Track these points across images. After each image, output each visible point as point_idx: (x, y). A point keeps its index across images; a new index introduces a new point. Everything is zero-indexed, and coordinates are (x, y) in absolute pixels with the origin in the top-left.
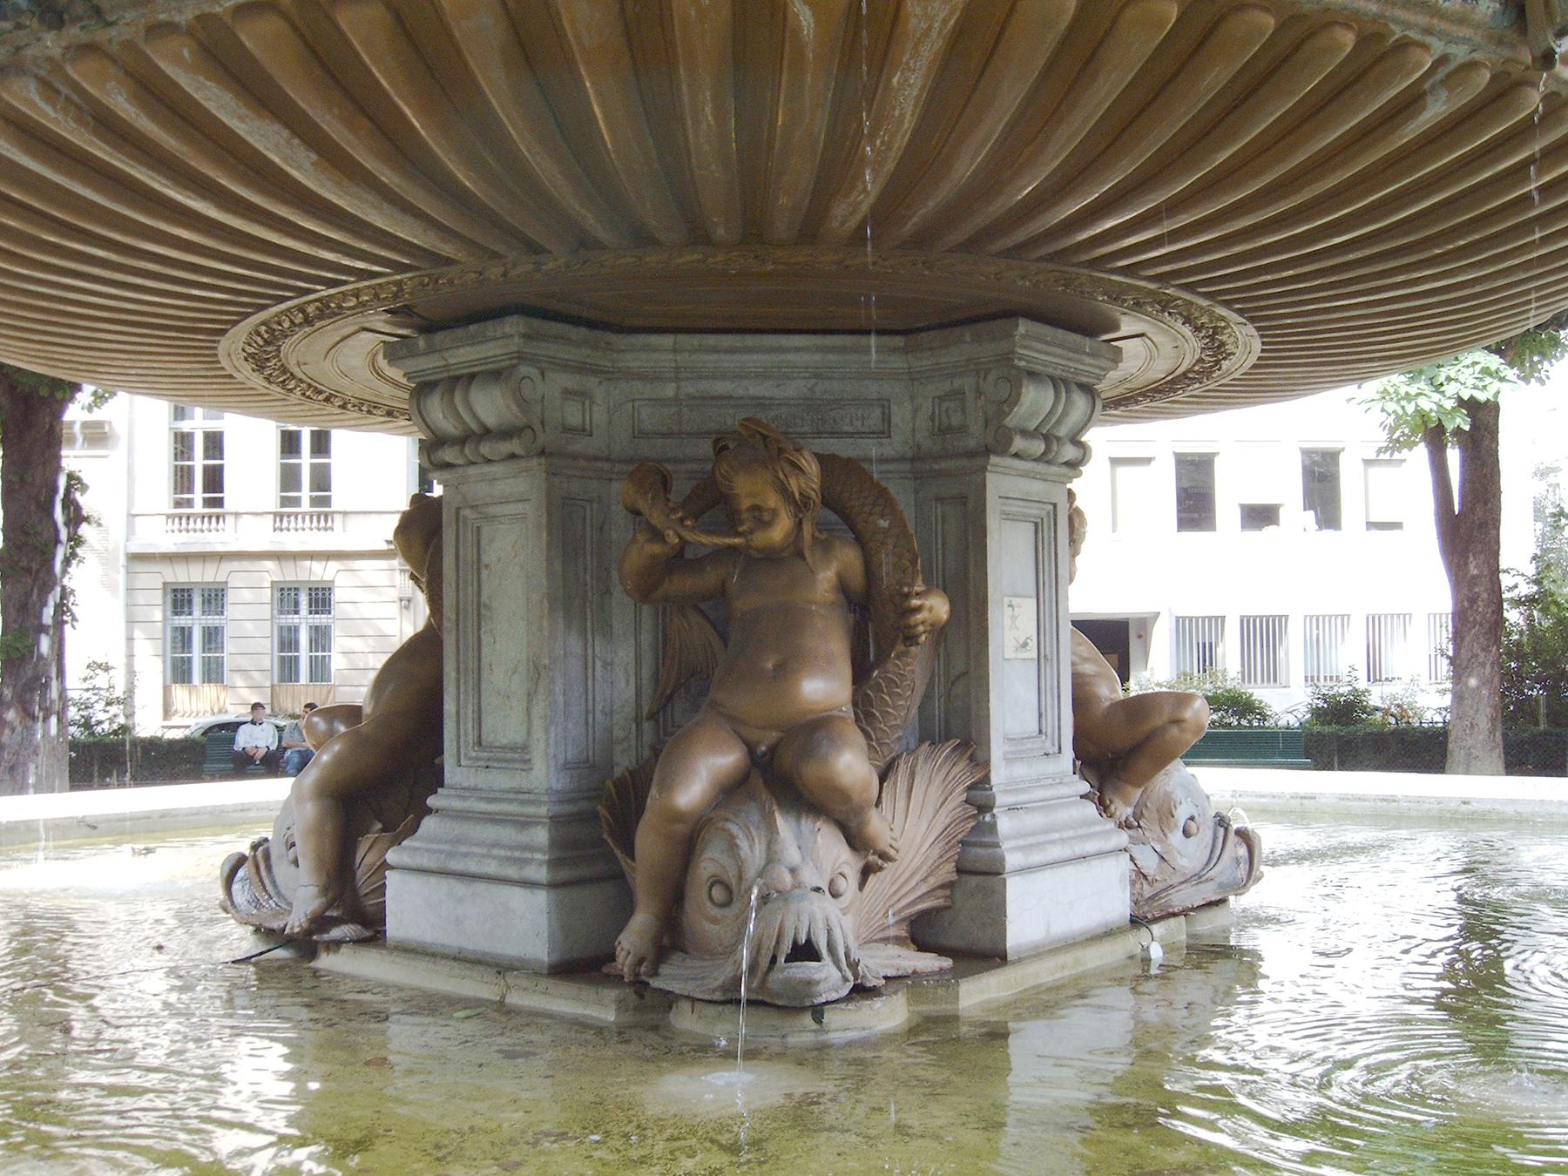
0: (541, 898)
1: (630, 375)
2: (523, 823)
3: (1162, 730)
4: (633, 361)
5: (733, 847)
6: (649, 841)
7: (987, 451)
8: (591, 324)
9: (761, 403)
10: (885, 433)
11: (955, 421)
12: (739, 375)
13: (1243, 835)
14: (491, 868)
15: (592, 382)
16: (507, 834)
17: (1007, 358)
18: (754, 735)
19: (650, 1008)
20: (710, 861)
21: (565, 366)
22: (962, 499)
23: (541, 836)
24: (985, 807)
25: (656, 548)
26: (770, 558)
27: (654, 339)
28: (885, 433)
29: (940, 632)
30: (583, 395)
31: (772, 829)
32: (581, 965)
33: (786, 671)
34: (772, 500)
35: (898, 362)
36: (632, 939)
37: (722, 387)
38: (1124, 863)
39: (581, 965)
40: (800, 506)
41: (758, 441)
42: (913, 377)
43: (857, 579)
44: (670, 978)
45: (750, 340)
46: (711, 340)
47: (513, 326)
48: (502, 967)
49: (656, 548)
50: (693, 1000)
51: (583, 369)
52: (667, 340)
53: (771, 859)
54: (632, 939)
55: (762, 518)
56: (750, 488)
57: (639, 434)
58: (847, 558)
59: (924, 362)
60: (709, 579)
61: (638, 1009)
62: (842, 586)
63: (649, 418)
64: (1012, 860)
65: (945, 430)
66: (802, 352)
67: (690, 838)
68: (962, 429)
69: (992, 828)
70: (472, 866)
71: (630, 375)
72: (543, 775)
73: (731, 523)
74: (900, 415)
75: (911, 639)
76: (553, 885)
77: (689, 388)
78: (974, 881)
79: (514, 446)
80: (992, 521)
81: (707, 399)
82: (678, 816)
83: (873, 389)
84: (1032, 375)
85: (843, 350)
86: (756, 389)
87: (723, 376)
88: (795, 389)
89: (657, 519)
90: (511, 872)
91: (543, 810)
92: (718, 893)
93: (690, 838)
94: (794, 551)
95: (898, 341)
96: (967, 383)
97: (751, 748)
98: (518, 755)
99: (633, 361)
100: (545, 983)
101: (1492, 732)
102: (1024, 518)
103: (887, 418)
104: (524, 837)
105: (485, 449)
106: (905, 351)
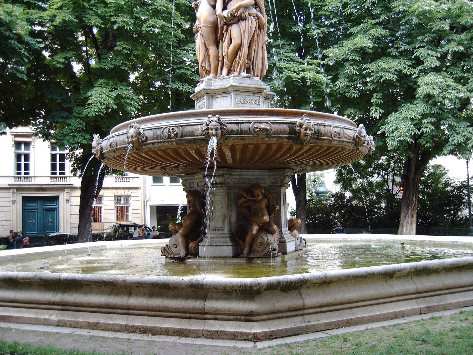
0: (231, 247)
1: (234, 175)
2: (224, 238)
3: (295, 224)
4: (234, 173)
5: (262, 238)
6: (248, 239)
7: (281, 186)
9: (250, 179)
10: (265, 183)
11: (275, 181)
13: (304, 239)
14: (221, 244)
16: (222, 239)
17: (284, 174)
18: (259, 224)
19: (250, 260)
20: (259, 240)
22: (277, 193)
23: (228, 239)
24: (282, 234)
25: (246, 200)
26: (258, 201)
27: (238, 170)
29: (278, 210)
31: (267, 236)
32: (237, 255)
33: (262, 216)
34: (260, 194)
35: (268, 173)
36: (246, 251)
37: (245, 177)
38: (294, 243)
39: (237, 255)
41: (257, 186)
42: (269, 175)
43: (267, 204)
44: (252, 256)
45: (250, 170)
46: (245, 170)
47: (225, 170)
48: (224, 258)
49: (246, 200)
50: (257, 258)
52: (239, 170)
53: (268, 239)
54: (246, 251)
55: (258, 196)
56: (258, 192)
57: (235, 183)
58: (266, 200)
59: (272, 173)
60: (248, 204)
61: (248, 260)
62: (266, 205)
64: (287, 241)
65: (274, 183)
66: (256, 172)
67: (254, 238)
68: (277, 183)
69: (283, 236)
70: (217, 244)
71: (234, 175)
72: (226, 231)
73: (253, 197)
74: (267, 181)
75: (275, 211)
76: (232, 246)
77: (241, 177)
78: (281, 244)
79: (224, 186)
81: (243, 178)
82: (253, 235)
83: (264, 177)
87: (245, 175)
88: (254, 177)
89: (246, 196)
90: (225, 244)
91: (228, 236)
92: (260, 244)
93: (254, 238)
94: (261, 200)
95: (268, 170)
96: (277, 177)
97: (259, 226)
98: (222, 228)
99: (234, 173)
100: (232, 259)
101: (305, 230)
103: (266, 181)
104: (225, 240)
105: (218, 186)
106: (269, 172)
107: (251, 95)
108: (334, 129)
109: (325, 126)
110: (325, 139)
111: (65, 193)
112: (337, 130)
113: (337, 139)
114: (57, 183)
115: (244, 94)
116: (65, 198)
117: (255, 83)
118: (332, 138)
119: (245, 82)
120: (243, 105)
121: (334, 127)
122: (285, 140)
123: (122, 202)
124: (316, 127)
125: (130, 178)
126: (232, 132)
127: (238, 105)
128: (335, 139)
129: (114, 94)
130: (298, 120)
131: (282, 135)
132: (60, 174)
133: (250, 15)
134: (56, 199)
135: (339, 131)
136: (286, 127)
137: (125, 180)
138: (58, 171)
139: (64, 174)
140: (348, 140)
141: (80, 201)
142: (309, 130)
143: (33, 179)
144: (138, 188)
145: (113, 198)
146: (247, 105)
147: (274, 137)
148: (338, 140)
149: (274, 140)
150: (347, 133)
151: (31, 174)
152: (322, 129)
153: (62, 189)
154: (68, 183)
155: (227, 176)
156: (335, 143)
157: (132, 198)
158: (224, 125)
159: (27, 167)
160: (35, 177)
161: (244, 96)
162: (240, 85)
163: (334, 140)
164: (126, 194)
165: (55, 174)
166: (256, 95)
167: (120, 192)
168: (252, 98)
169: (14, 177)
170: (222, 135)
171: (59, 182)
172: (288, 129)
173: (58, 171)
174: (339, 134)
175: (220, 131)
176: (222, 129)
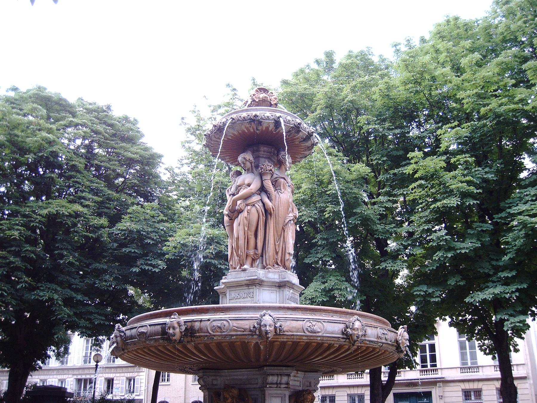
1: (223, 376)
4: (223, 374)
8: (214, 369)
9: (241, 379)
12: (237, 376)
15: (218, 377)
21: (212, 376)
28: (257, 384)
30: (216, 379)
35: (258, 373)
37: (235, 377)
40: (233, 397)
45: (237, 370)
51: (215, 376)
52: (226, 371)
63: (227, 382)
66: (244, 372)
71: (223, 376)
77: (232, 378)
80: (267, 398)
84: (269, 375)
85: (249, 371)
86: (241, 377)
88: (245, 377)
95: (257, 369)
102: (278, 397)
106: (258, 371)
107: (245, 288)
108: (214, 322)
109: (201, 321)
110: (202, 336)
111: (438, 389)
112: (218, 324)
113: (217, 334)
114: (428, 376)
115: (237, 289)
116: (438, 394)
117: (249, 275)
118: (209, 332)
119: (239, 276)
120: (237, 300)
121: (214, 320)
122: (161, 341)
123: (473, 398)
124: (189, 324)
125: (478, 367)
126: (132, 337)
127: (232, 301)
128: (215, 334)
129: (323, 287)
130: (167, 320)
131: (156, 337)
132: (431, 366)
133: (247, 205)
134: (428, 395)
135: (219, 325)
136: (159, 328)
137: (475, 370)
138: (429, 364)
139: (436, 366)
140: (239, 333)
141: (370, 400)
142: (171, 329)
143: (480, 368)
144: (524, 378)
145: (460, 394)
146: (241, 300)
147: (151, 340)
148: (221, 335)
149: (152, 342)
150: (235, 325)
151: (438, 366)
152: (197, 325)
153: (434, 383)
154: (439, 375)
155: (214, 378)
156: (219, 338)
157: (484, 393)
158: (123, 332)
159: (433, 358)
160: (441, 369)
161: (239, 291)
162: (236, 280)
163: (214, 336)
164: (359, 392)
165: (426, 366)
166: (250, 287)
167: (467, 386)
168: (246, 291)
169: (461, 368)
170: (122, 340)
171: (431, 376)
172: (160, 329)
173: (429, 364)
174: (220, 328)
175: (119, 339)
176: (121, 335)
